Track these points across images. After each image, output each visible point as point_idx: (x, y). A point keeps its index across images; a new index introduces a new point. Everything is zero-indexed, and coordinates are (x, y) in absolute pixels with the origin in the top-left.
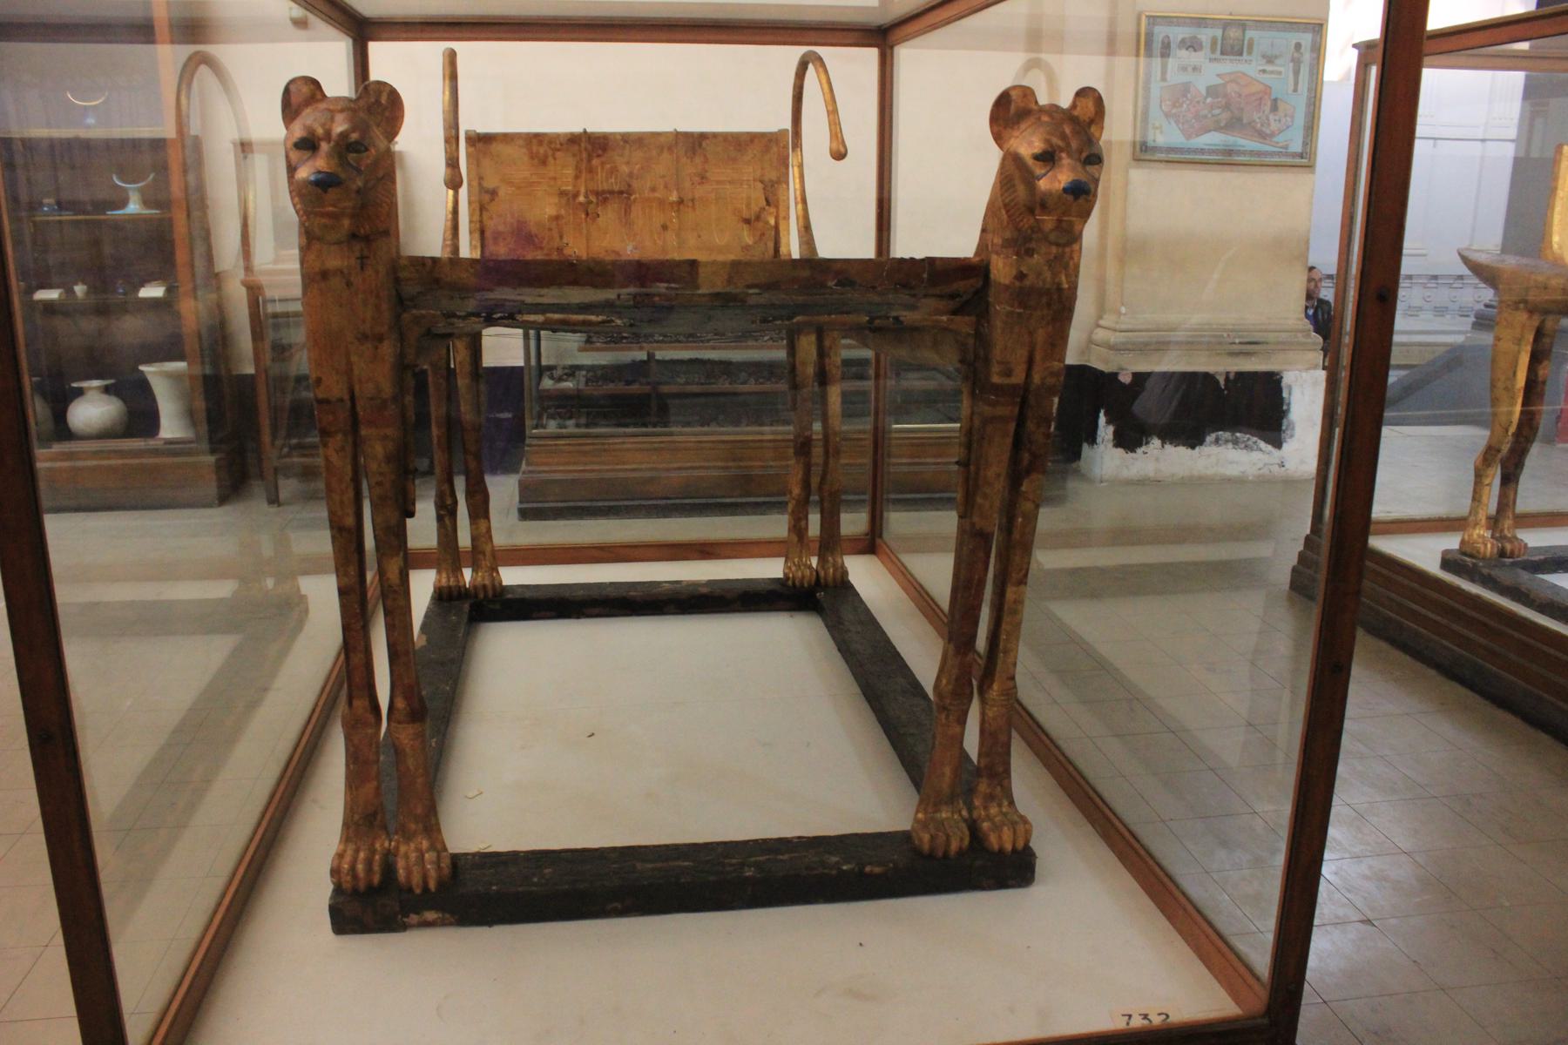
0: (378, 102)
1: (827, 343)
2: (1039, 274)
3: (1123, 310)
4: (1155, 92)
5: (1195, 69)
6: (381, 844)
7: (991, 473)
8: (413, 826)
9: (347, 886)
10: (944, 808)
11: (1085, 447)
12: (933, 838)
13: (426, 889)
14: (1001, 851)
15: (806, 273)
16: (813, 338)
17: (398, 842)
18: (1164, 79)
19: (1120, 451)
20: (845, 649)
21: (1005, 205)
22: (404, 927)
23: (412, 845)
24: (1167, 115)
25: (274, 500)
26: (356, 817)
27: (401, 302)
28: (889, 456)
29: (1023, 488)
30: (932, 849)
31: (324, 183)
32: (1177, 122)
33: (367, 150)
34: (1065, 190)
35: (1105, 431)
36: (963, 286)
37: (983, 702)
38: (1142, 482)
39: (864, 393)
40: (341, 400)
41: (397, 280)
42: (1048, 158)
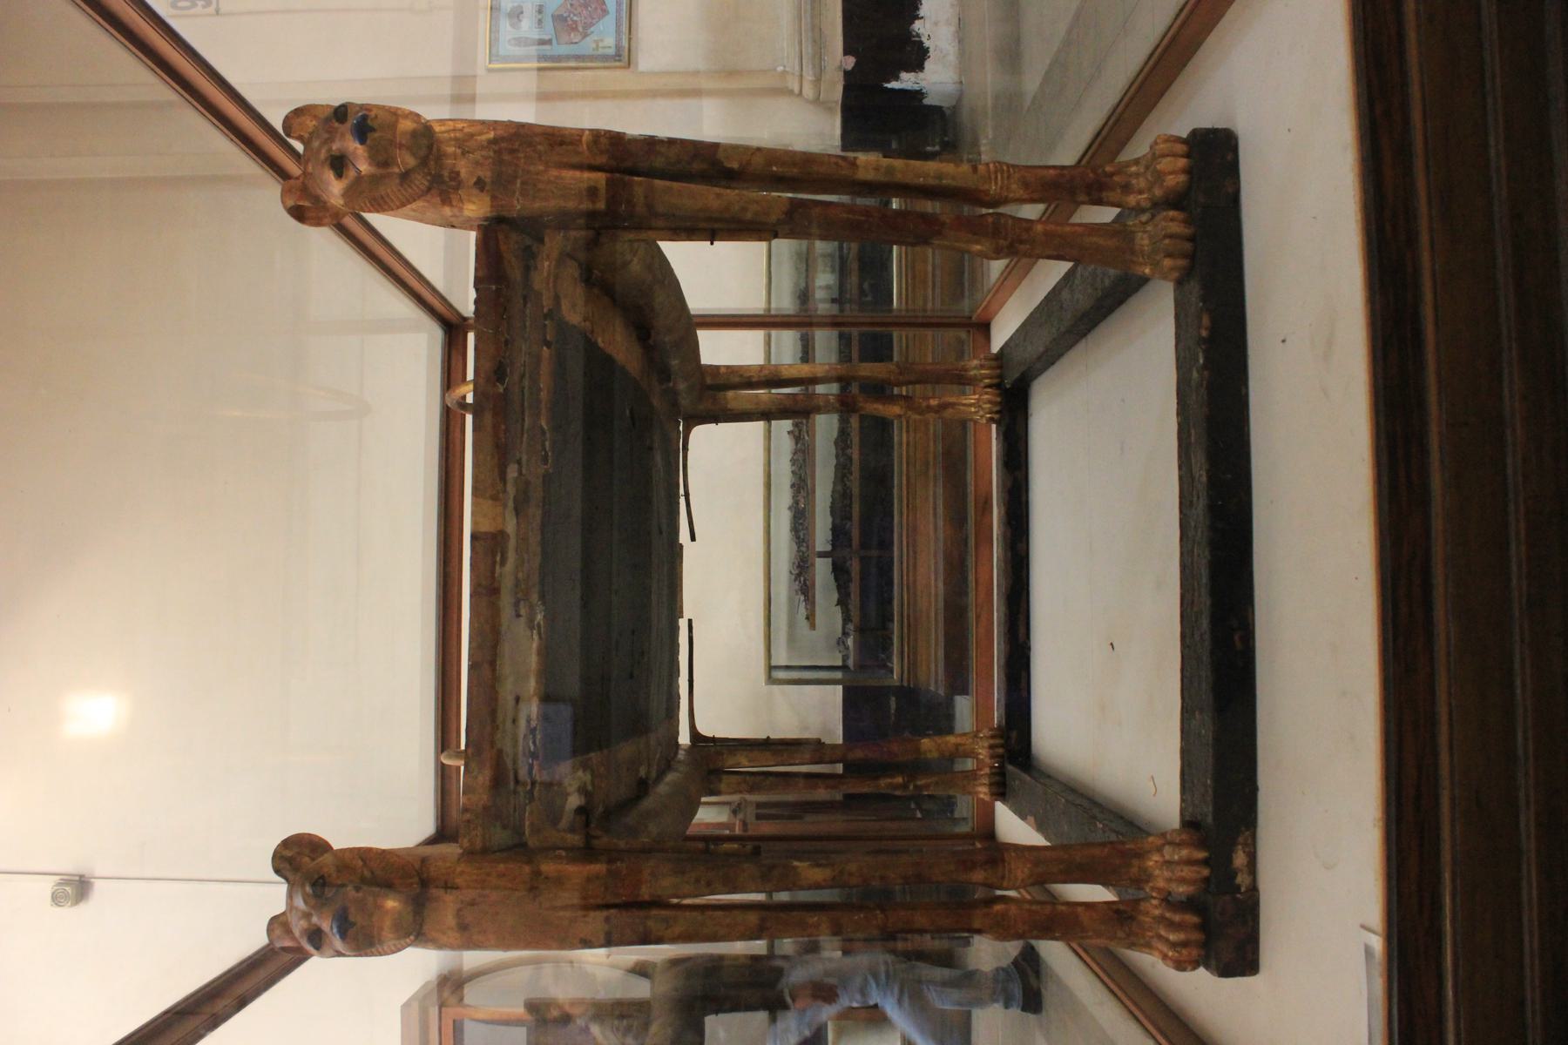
0: (290, 860)
1: (737, 380)
2: (477, 163)
3: (780, 69)
4: (563, 50)
5: (540, 12)
6: (1154, 908)
7: (715, 204)
8: (1134, 870)
9: (1195, 952)
10: (1138, 241)
11: (927, 101)
12: (1169, 255)
13: (1205, 862)
14: (1188, 171)
15: (488, 419)
16: (730, 394)
17: (1153, 889)
18: (549, 42)
19: (927, 64)
20: (1049, 358)
21: (403, 205)
22: (1254, 889)
23: (1157, 872)
24: (585, 36)
25: (967, 943)
26: (1120, 934)
27: (519, 849)
28: (925, 310)
29: (735, 166)
30: (1184, 256)
31: (345, 927)
32: (592, 25)
33: (322, 877)
34: (363, 141)
35: (906, 81)
36: (510, 244)
37: (1005, 201)
38: (961, 38)
39: (861, 335)
40: (607, 920)
41: (485, 851)
42: (339, 164)
